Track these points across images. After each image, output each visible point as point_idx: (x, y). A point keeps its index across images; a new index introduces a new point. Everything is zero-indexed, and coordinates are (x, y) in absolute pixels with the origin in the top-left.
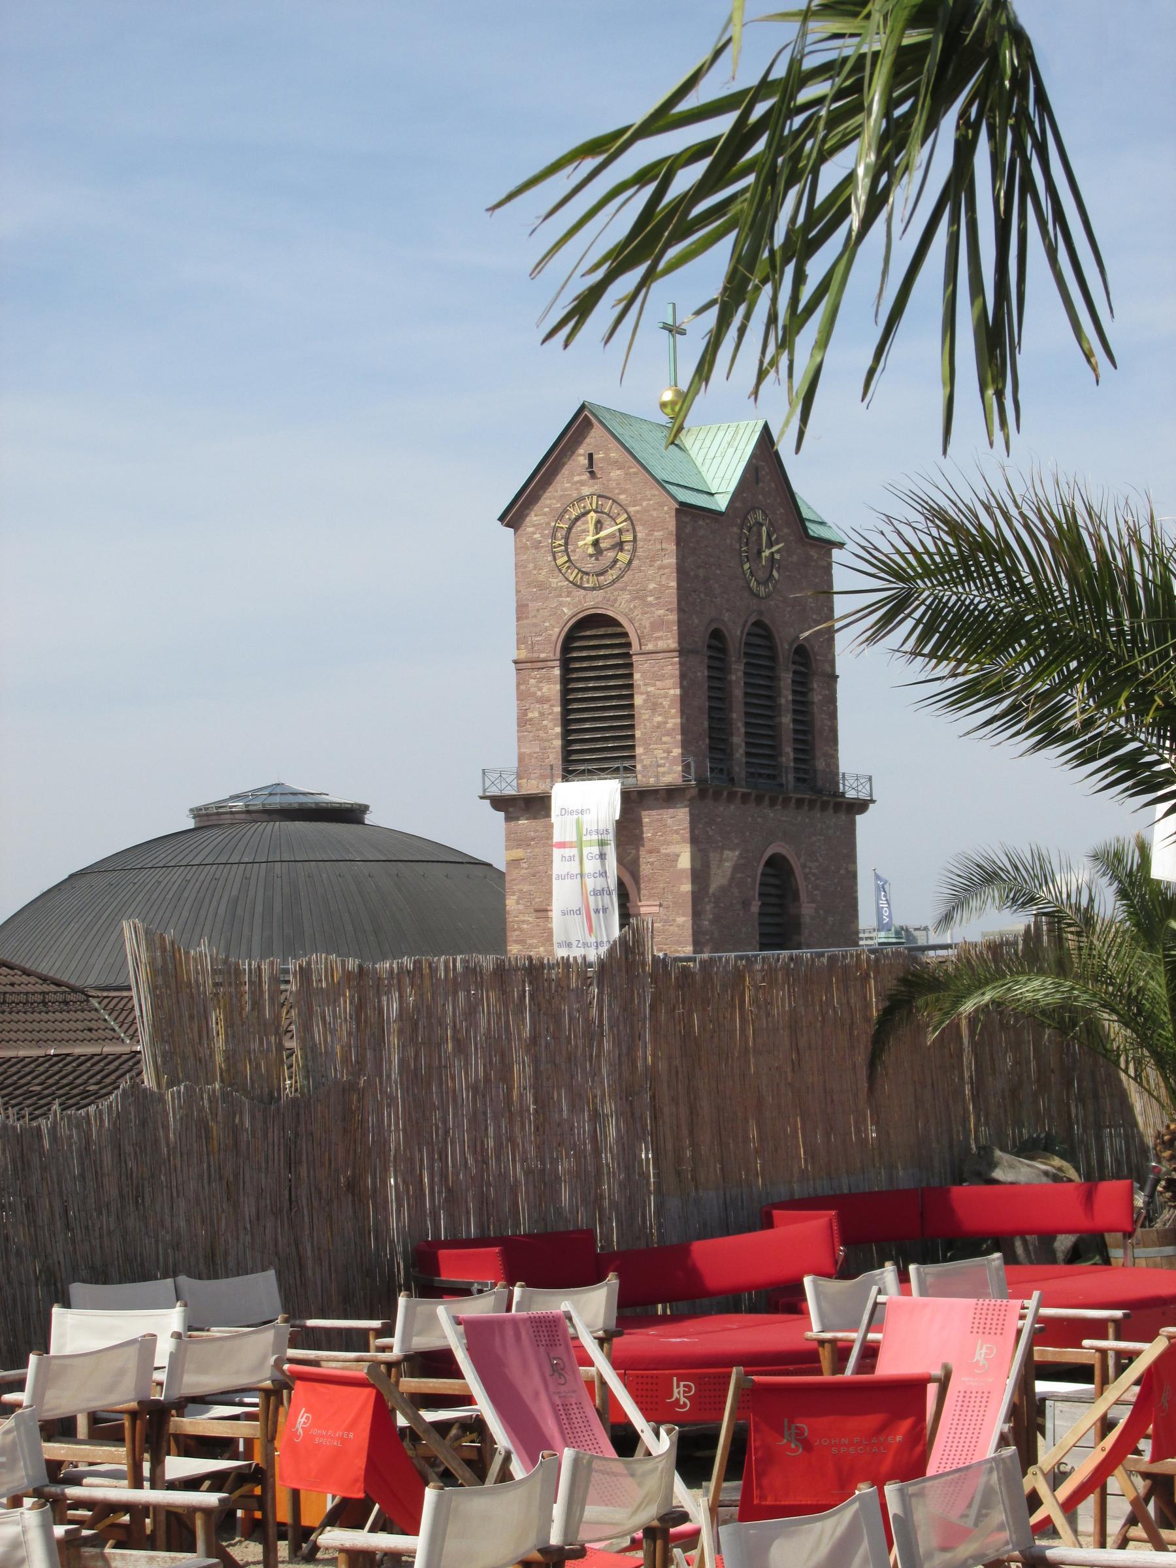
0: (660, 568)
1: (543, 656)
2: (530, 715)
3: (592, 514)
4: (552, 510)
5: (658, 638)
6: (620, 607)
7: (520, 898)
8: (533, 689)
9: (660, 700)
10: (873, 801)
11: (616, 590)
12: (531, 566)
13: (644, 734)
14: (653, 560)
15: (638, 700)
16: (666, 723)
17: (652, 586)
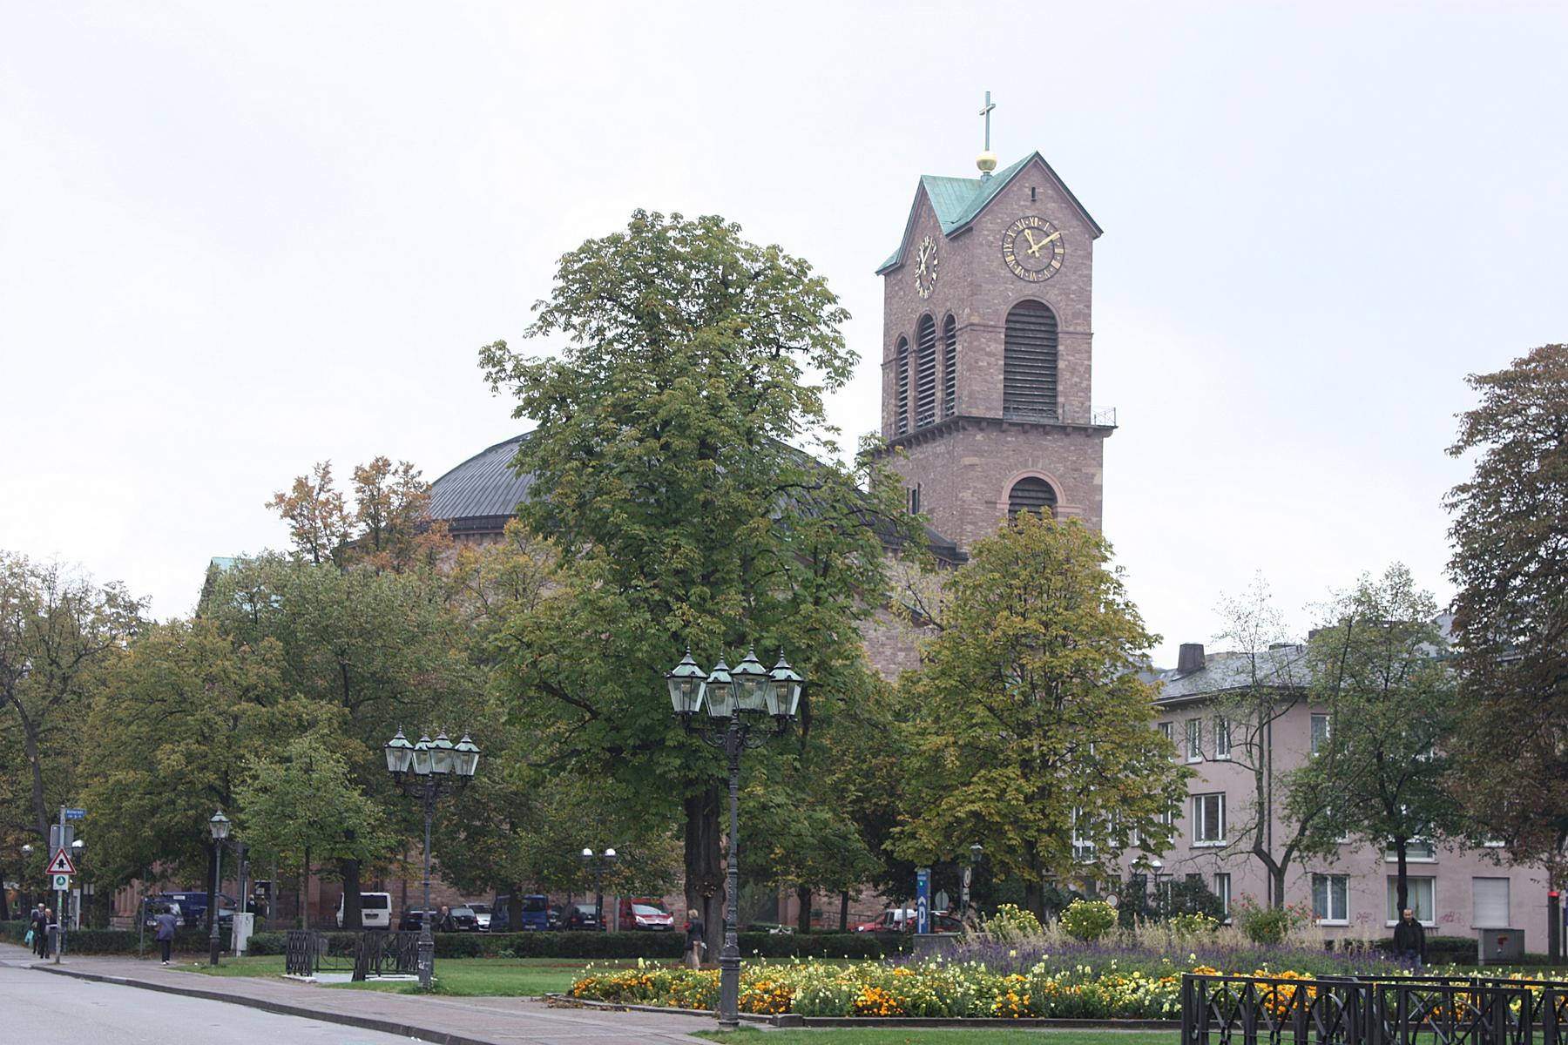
0: (1081, 276)
1: (992, 323)
2: (981, 364)
3: (1027, 231)
4: (1003, 222)
5: (1077, 324)
6: (1052, 297)
7: (974, 492)
8: (983, 346)
9: (1077, 367)
10: (1116, 427)
11: (1048, 285)
12: (984, 258)
13: (1065, 388)
14: (1076, 269)
15: (1061, 365)
16: (1081, 383)
17: (1074, 287)
